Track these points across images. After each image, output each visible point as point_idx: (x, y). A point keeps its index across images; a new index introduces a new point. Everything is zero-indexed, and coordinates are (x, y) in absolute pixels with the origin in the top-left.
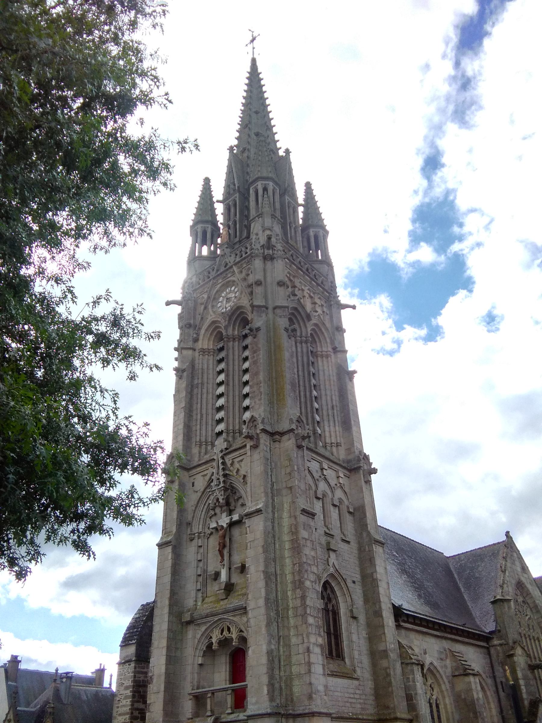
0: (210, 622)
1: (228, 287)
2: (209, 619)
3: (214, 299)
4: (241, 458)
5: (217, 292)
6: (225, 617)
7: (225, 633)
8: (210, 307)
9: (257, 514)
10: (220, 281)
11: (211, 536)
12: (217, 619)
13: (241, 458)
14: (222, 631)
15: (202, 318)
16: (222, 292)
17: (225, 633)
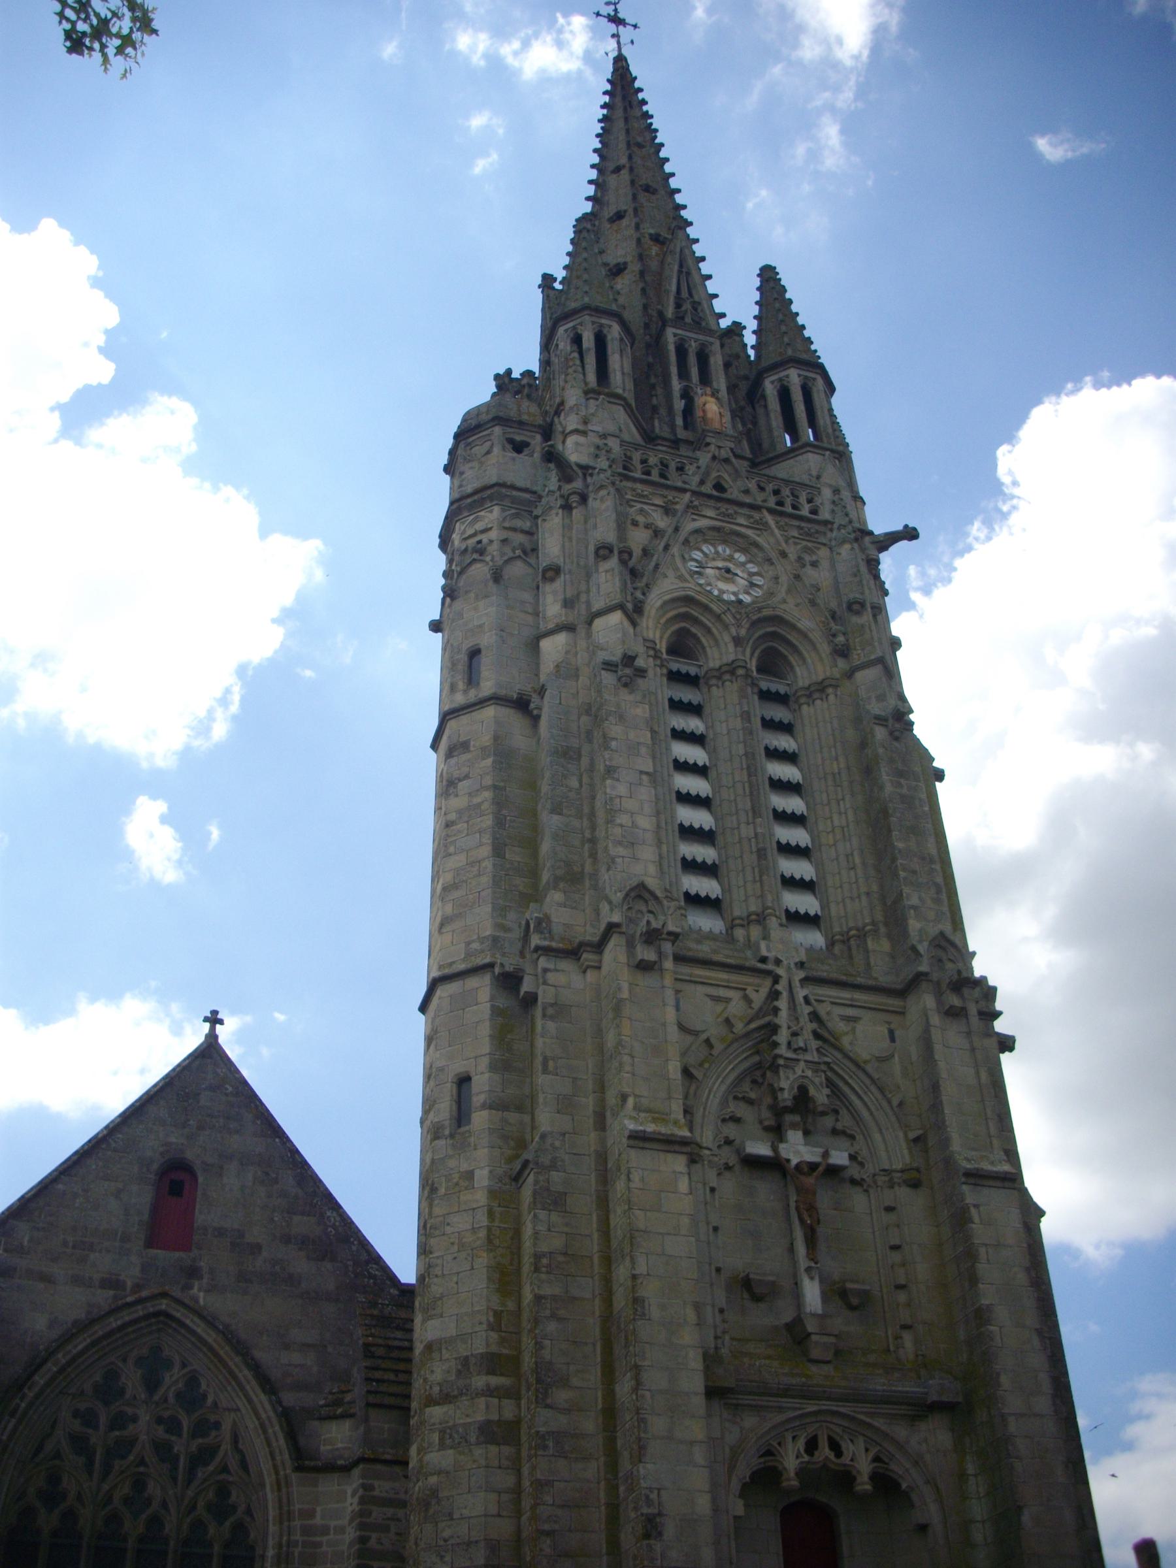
0: (780, 1409)
1: (725, 542)
2: (786, 1402)
3: (686, 542)
4: (850, 1012)
5: (697, 531)
6: (842, 1410)
7: (824, 1452)
8: (675, 550)
9: (999, 1184)
10: (710, 513)
11: (727, 1174)
12: (815, 1408)
13: (850, 1012)
14: (812, 1446)
15: (657, 566)
16: (706, 541)
17: (824, 1452)
